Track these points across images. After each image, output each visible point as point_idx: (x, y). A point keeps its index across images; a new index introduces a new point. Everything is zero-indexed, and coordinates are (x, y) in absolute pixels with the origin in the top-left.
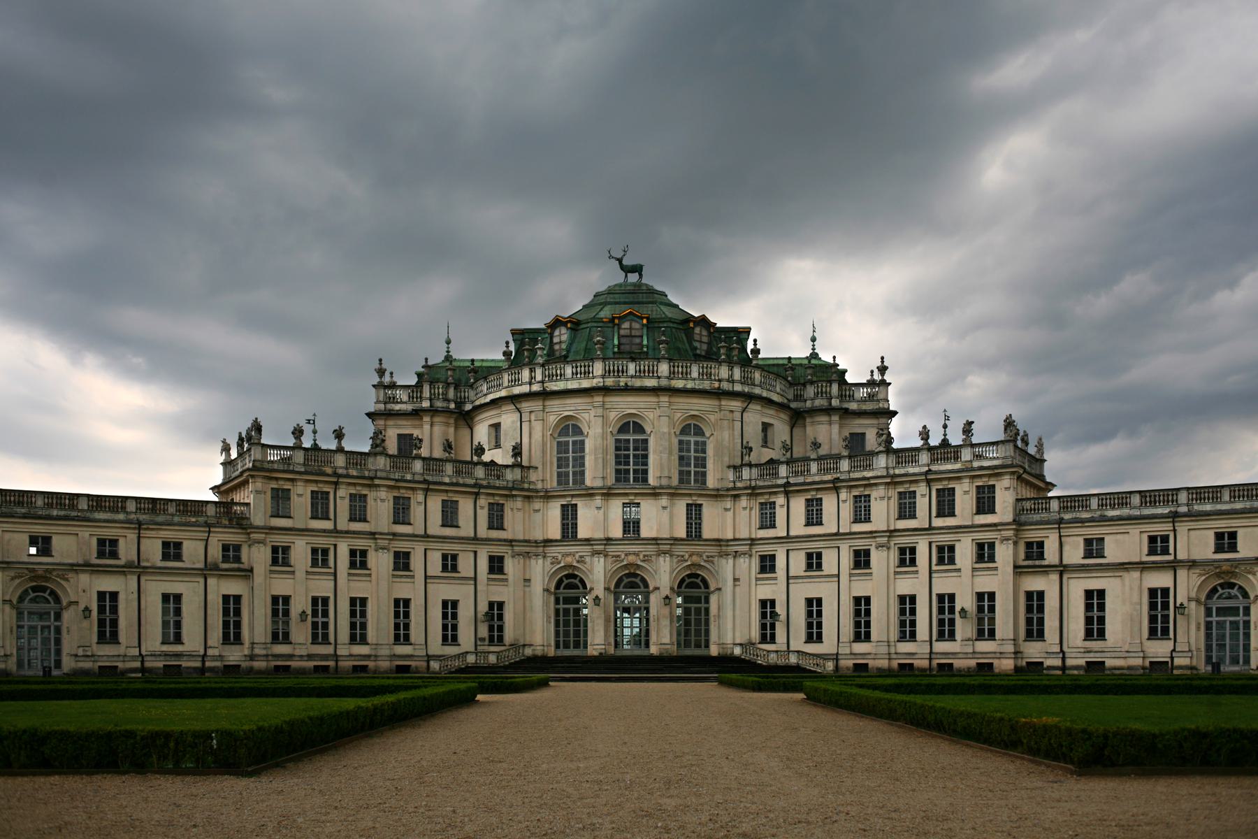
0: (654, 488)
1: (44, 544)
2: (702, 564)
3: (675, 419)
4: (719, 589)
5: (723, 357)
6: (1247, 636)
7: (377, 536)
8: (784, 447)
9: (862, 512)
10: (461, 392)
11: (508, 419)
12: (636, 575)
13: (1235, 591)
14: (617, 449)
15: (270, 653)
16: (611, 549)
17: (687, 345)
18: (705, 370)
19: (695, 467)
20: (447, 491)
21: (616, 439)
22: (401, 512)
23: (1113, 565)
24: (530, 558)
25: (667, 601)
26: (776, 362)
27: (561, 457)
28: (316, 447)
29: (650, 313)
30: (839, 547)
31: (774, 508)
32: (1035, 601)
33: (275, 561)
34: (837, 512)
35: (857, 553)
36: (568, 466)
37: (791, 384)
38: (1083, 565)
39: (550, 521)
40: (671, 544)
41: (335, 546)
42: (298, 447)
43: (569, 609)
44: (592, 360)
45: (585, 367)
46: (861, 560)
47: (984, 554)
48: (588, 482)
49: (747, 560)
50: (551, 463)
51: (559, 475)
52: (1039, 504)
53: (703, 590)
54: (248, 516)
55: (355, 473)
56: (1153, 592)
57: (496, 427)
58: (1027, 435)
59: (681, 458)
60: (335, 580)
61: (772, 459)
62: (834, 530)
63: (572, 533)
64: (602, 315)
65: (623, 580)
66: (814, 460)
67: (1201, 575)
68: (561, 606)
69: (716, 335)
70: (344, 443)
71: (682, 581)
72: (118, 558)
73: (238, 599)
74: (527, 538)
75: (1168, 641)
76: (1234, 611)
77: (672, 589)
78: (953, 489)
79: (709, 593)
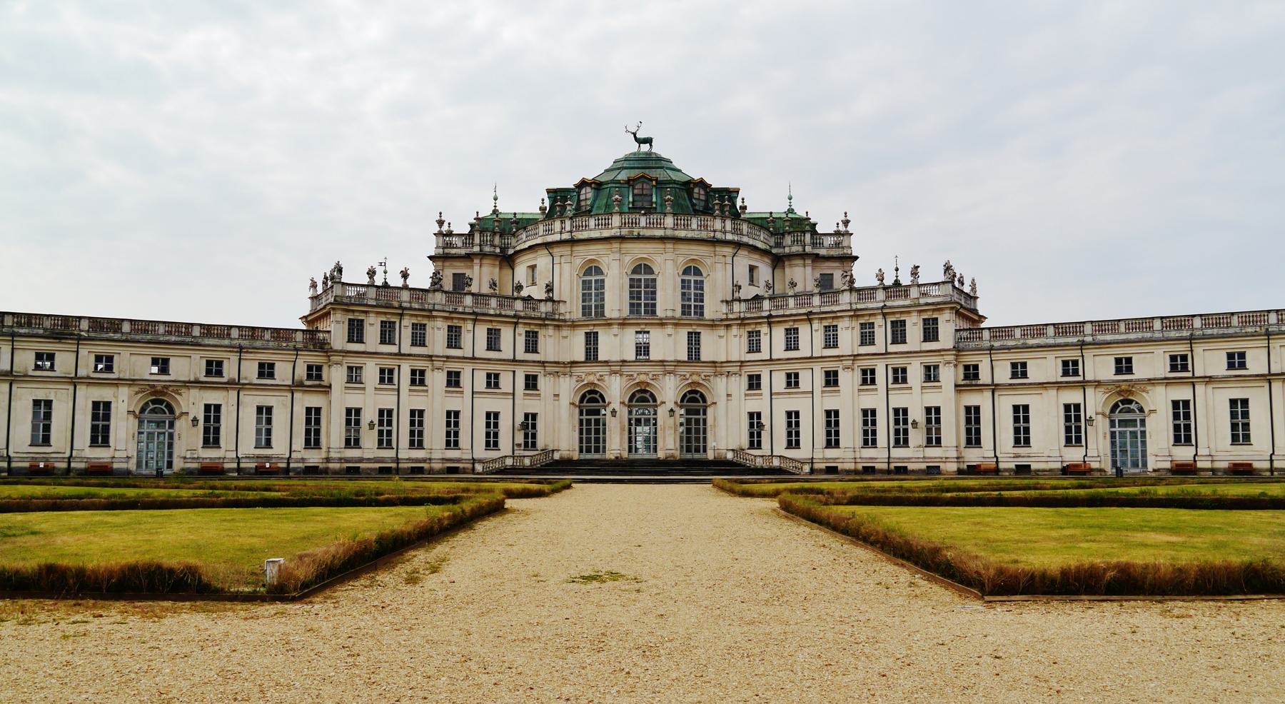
0: (661, 319)
1: (163, 365)
2: (701, 382)
3: (678, 263)
4: (715, 403)
5: (717, 212)
6: (1144, 443)
7: (433, 359)
8: (767, 286)
9: (831, 342)
10: (505, 239)
11: (542, 260)
12: (645, 391)
13: (1133, 406)
14: (631, 286)
16: (625, 369)
17: (688, 202)
18: (703, 223)
19: (695, 302)
20: (491, 321)
21: (630, 279)
22: (454, 339)
23: (1035, 384)
24: (559, 376)
25: (672, 413)
26: (760, 216)
28: (386, 285)
29: (658, 176)
30: (812, 369)
31: (760, 336)
32: (973, 415)
33: (350, 380)
34: (811, 339)
35: (828, 374)
37: (772, 234)
38: (1010, 385)
39: (575, 346)
40: (675, 366)
41: (399, 366)
42: (371, 285)
43: (591, 420)
44: (611, 214)
45: (605, 219)
46: (831, 379)
47: (930, 375)
48: (608, 314)
49: (738, 379)
50: (578, 298)
51: (584, 307)
52: (973, 333)
53: (701, 403)
54: (329, 341)
55: (416, 306)
56: (1067, 407)
57: (533, 267)
59: (683, 294)
60: (399, 395)
61: (757, 295)
62: (809, 355)
64: (619, 177)
65: (586, 396)
66: (792, 296)
67: (1105, 393)
68: (584, 417)
69: (712, 194)
70: (408, 282)
71: (685, 396)
73: (318, 410)
74: (556, 360)
75: (1081, 448)
76: (1132, 423)
77: (676, 403)
78: (904, 321)
79: (706, 407)
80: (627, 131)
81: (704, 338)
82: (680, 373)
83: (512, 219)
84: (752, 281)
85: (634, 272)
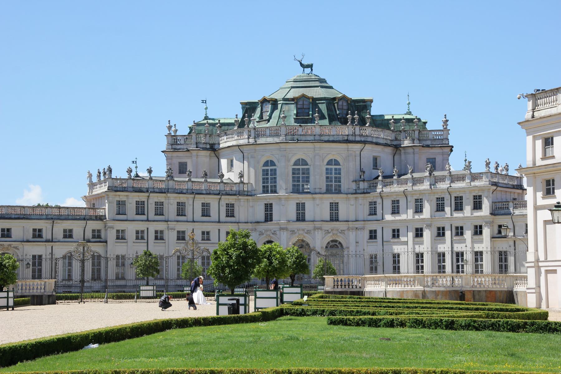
14: (293, 173)
15: (114, 284)
17: (334, 112)
19: (335, 182)
27: (265, 178)
36: (268, 182)
41: (148, 228)
51: (264, 187)
58: (508, 166)
59: (327, 178)
63: (270, 218)
70: (152, 175)
72: (42, 238)
80: (295, 59)
81: (341, 207)
82: (325, 229)
83: (217, 124)
84: (376, 166)
85: (295, 164)
